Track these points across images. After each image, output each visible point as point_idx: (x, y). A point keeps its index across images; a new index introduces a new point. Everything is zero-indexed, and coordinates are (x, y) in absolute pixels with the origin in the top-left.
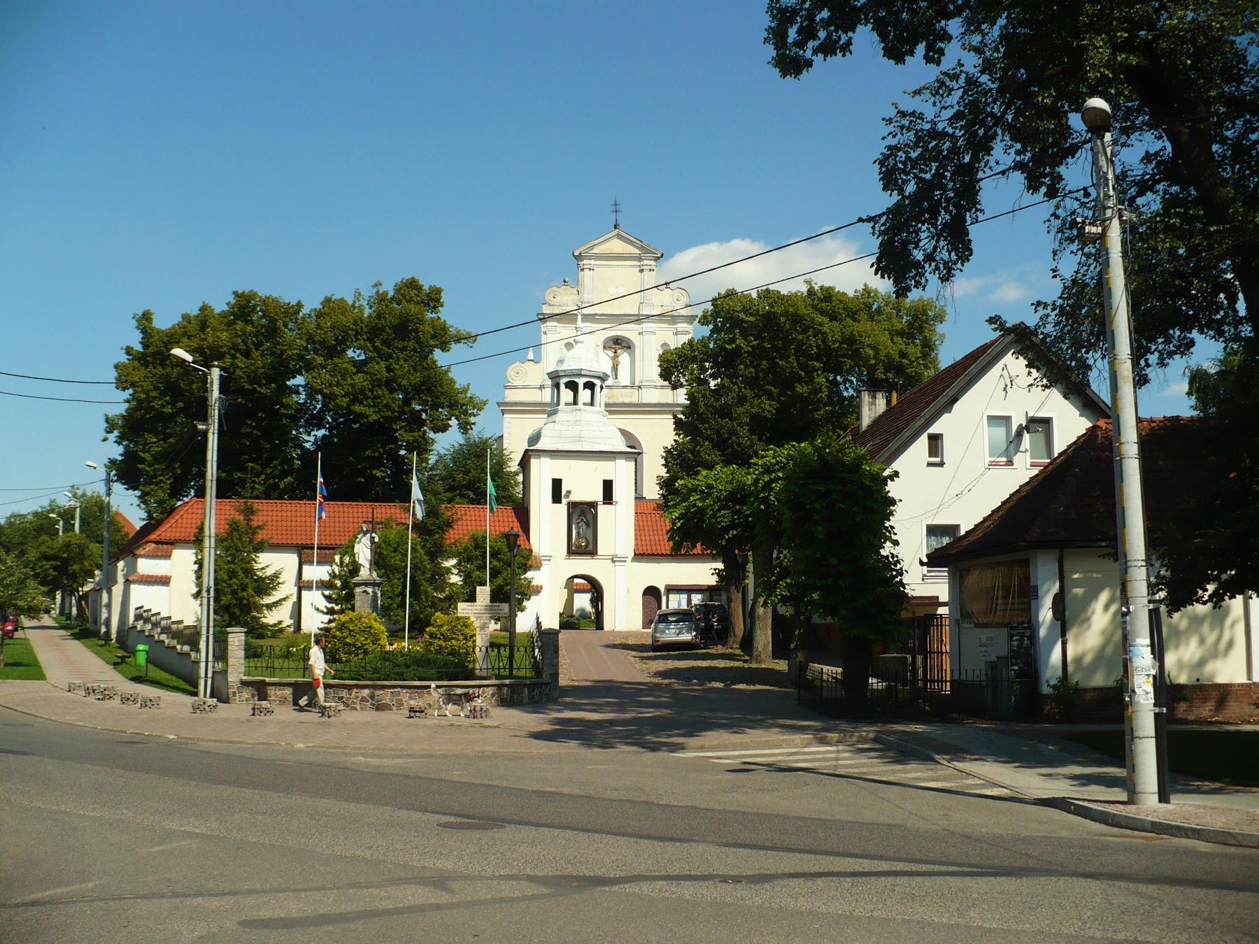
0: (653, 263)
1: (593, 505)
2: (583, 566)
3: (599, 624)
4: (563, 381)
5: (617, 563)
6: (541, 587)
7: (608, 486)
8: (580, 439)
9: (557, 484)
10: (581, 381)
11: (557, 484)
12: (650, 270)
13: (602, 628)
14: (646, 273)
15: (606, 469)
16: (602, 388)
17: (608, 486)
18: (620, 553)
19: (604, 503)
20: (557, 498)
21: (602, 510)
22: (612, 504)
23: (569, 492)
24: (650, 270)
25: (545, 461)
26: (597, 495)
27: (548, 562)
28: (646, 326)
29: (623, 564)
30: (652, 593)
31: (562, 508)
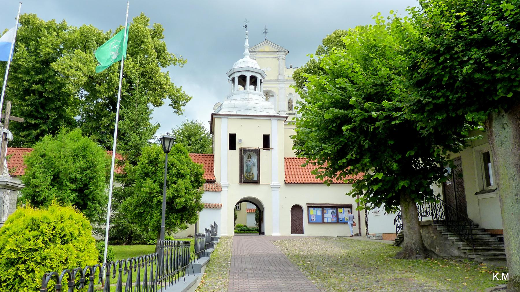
0: (284, 56)
1: (256, 151)
2: (250, 191)
3: (259, 230)
4: (236, 76)
5: (273, 189)
6: (221, 206)
7: (266, 139)
8: (248, 108)
9: (232, 138)
10: (248, 75)
11: (232, 138)
12: (283, 59)
13: (263, 234)
14: (281, 61)
15: (266, 127)
16: (261, 82)
17: (266, 139)
18: (275, 183)
19: (264, 149)
20: (232, 145)
21: (263, 153)
22: (269, 150)
23: (240, 141)
24: (283, 59)
25: (224, 120)
26: (260, 144)
27: (226, 189)
28: (281, 85)
29: (278, 190)
30: (296, 209)
31: (236, 153)
